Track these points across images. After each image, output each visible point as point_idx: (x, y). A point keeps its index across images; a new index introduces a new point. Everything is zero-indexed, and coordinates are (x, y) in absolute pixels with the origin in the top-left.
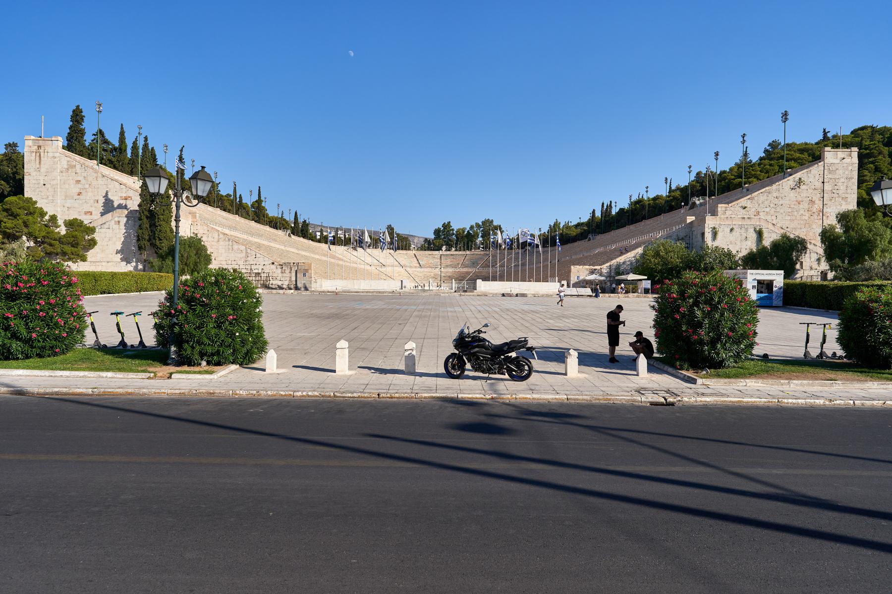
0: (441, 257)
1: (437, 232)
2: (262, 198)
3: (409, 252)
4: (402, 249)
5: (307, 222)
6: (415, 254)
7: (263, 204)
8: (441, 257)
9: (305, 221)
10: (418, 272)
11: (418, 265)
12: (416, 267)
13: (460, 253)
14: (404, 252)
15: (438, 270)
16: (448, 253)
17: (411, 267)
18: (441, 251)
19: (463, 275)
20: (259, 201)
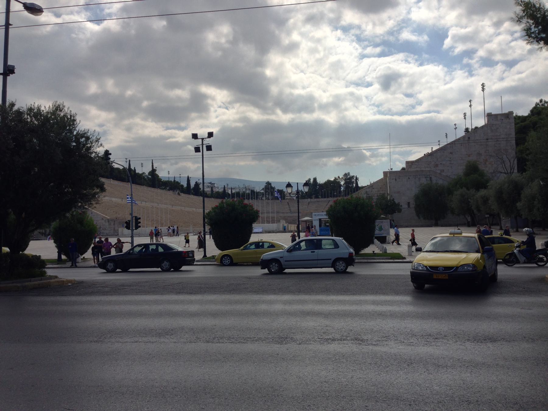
2: (154, 168)
6: (288, 203)
7: (157, 172)
10: (288, 216)
11: (289, 211)
12: (287, 213)
17: (283, 213)
18: (309, 199)
20: (153, 171)
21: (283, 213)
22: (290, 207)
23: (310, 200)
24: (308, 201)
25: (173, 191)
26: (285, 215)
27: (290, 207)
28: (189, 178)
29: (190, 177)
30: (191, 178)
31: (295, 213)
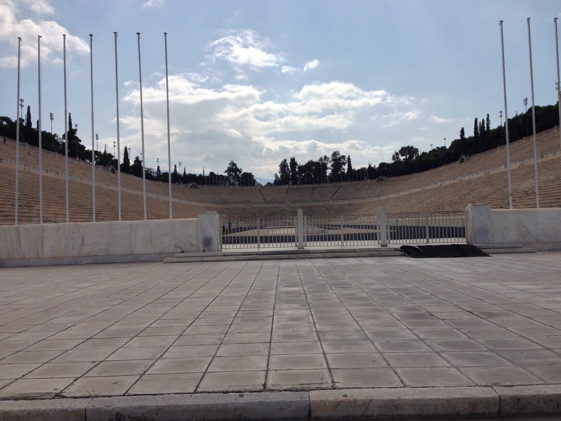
0: (287, 192)
1: (283, 166)
3: (253, 187)
4: (246, 185)
5: (140, 159)
6: (260, 190)
8: (287, 192)
9: (137, 158)
10: (264, 208)
11: (264, 201)
13: (308, 186)
14: (249, 188)
15: (285, 205)
16: (296, 186)
17: (256, 203)
18: (287, 186)
19: (313, 210)
21: (256, 203)
22: (263, 196)
23: (288, 187)
24: (285, 188)
25: (104, 167)
26: (260, 206)
27: (263, 196)
28: (128, 150)
29: (130, 149)
30: (130, 150)
31: (271, 203)
